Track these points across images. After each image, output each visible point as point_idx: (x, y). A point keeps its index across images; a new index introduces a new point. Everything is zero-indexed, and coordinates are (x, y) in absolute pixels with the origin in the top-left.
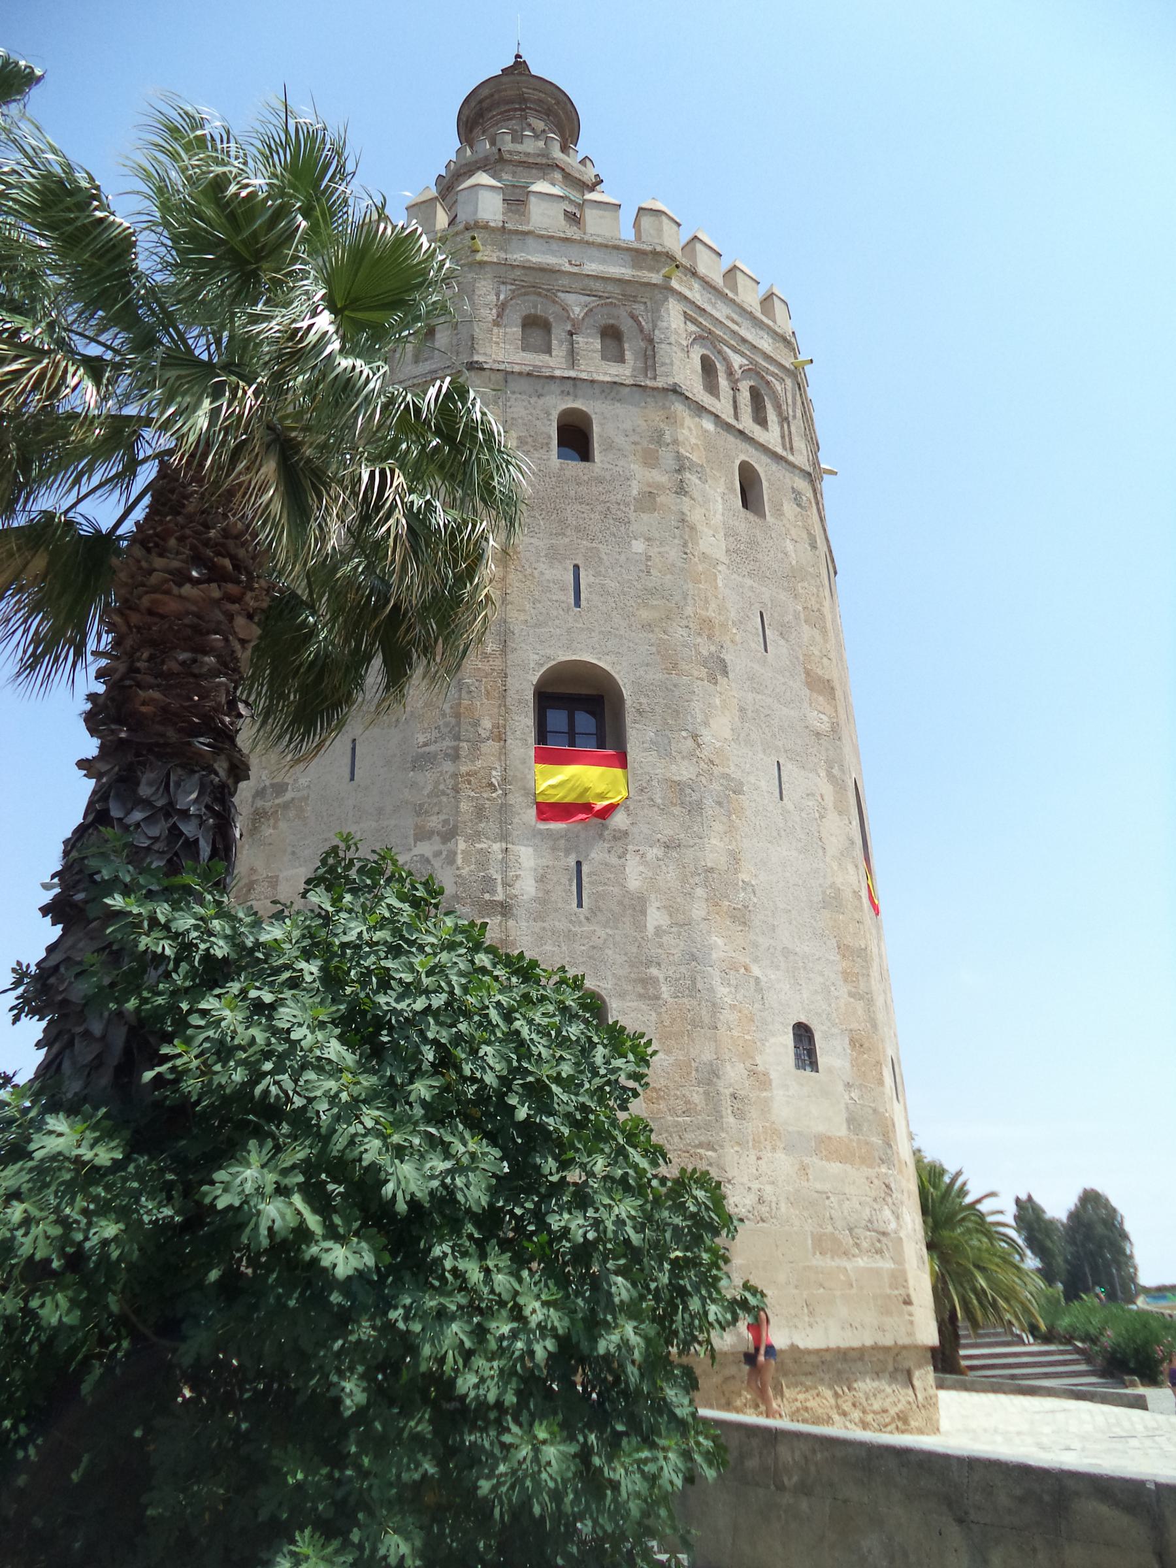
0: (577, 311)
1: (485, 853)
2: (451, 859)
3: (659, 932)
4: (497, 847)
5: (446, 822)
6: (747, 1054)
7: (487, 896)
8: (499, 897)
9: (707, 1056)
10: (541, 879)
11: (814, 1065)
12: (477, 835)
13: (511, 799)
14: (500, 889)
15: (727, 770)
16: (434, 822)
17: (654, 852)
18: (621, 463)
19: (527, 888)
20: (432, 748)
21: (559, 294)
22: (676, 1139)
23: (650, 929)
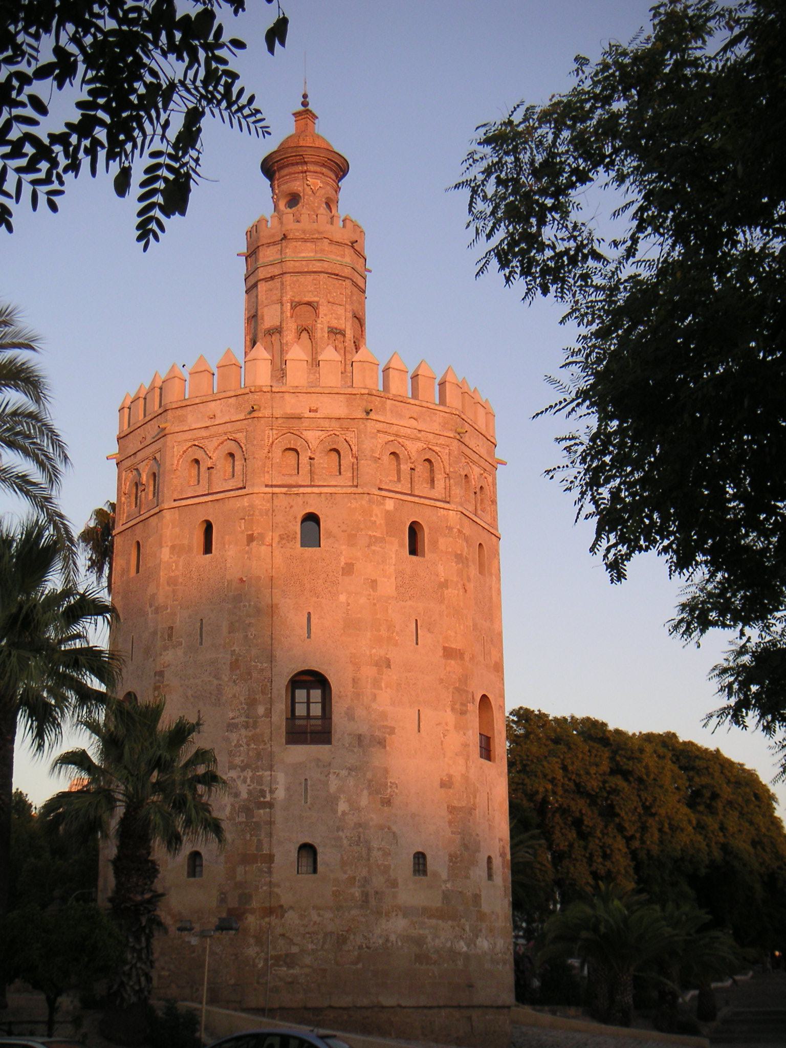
0: (314, 444)
1: (261, 777)
2: (245, 781)
3: (344, 813)
4: (268, 773)
5: (243, 761)
6: (386, 870)
7: (262, 799)
8: (268, 799)
9: (364, 873)
10: (288, 789)
11: (425, 873)
12: (257, 769)
13: (274, 749)
14: (268, 796)
15: (385, 723)
16: (237, 761)
17: (344, 773)
18: (336, 546)
19: (280, 794)
20: (236, 721)
21: (304, 433)
22: (346, 914)
23: (340, 813)
